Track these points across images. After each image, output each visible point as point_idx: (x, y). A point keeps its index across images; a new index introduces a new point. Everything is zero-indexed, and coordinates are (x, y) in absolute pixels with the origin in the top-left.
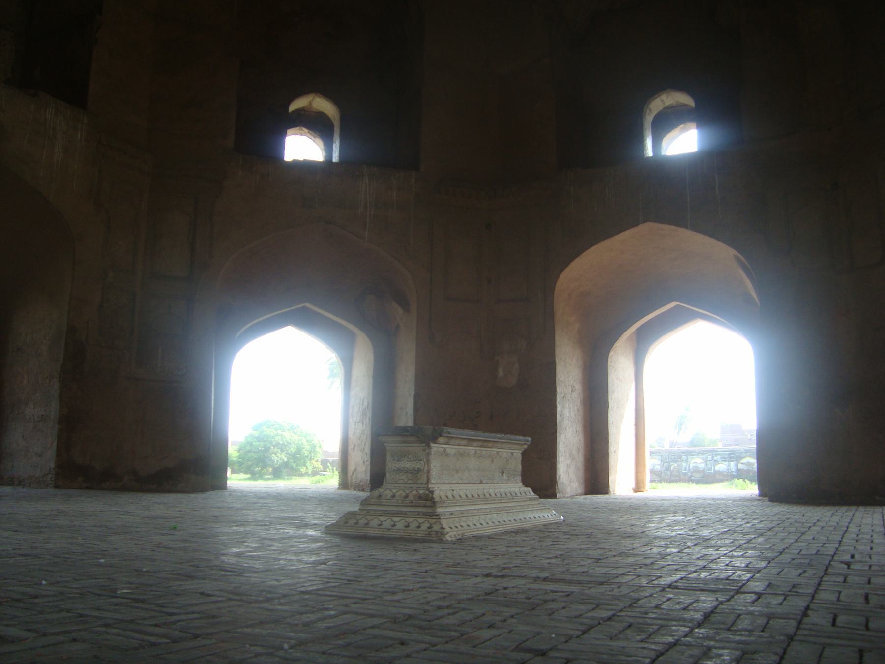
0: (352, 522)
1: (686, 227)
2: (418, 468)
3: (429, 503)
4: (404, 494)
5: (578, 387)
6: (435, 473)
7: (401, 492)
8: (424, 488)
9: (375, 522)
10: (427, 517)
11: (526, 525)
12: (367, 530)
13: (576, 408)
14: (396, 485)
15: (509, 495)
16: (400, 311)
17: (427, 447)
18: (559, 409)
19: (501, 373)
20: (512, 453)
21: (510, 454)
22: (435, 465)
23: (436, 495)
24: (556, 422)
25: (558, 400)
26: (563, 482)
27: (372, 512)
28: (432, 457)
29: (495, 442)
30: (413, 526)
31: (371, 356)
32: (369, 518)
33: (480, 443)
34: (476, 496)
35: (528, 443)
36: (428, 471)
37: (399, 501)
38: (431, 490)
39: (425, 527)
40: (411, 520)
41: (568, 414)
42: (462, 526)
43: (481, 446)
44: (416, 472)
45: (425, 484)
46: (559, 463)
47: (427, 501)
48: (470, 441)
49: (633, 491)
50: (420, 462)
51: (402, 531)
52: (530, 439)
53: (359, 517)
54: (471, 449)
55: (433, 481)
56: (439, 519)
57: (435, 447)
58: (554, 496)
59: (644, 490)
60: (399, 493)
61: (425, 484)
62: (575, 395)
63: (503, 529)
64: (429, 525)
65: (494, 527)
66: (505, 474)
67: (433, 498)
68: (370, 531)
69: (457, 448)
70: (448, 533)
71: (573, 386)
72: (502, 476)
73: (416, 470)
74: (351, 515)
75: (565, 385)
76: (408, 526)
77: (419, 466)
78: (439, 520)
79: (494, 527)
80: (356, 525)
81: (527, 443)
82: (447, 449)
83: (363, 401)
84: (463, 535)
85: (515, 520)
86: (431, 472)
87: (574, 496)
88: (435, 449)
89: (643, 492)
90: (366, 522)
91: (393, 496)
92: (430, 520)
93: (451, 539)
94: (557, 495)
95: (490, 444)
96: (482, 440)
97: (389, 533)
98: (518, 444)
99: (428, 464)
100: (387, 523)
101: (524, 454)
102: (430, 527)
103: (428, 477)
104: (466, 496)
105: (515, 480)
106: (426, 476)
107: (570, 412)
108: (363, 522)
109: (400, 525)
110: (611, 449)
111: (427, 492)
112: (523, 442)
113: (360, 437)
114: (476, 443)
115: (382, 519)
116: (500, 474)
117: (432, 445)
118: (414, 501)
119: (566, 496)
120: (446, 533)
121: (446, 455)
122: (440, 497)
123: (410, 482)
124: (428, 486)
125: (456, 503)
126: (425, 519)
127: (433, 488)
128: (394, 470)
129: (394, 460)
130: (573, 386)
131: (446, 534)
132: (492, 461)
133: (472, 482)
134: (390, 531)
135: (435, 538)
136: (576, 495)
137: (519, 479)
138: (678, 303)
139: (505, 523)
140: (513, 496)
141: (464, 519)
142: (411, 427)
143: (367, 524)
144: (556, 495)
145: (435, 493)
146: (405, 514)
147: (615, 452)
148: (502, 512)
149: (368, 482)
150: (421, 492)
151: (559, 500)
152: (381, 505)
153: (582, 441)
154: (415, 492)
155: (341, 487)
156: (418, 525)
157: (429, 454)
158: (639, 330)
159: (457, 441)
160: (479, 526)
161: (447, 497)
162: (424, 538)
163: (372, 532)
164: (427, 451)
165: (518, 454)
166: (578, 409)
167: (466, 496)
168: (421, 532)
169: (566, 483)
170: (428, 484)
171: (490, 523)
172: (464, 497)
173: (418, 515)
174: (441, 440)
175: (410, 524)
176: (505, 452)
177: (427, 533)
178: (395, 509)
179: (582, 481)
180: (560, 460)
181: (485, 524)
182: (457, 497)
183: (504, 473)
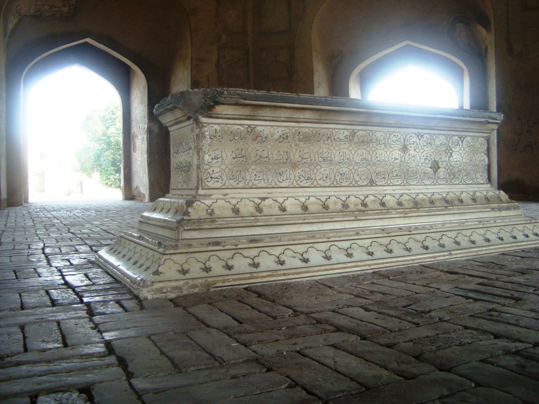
16: (484, 31)
28: (206, 142)
36: (198, 167)
69: (294, 127)
105: (472, 179)
117: (204, 120)
124: (197, 192)
157: (200, 137)
164: (197, 131)
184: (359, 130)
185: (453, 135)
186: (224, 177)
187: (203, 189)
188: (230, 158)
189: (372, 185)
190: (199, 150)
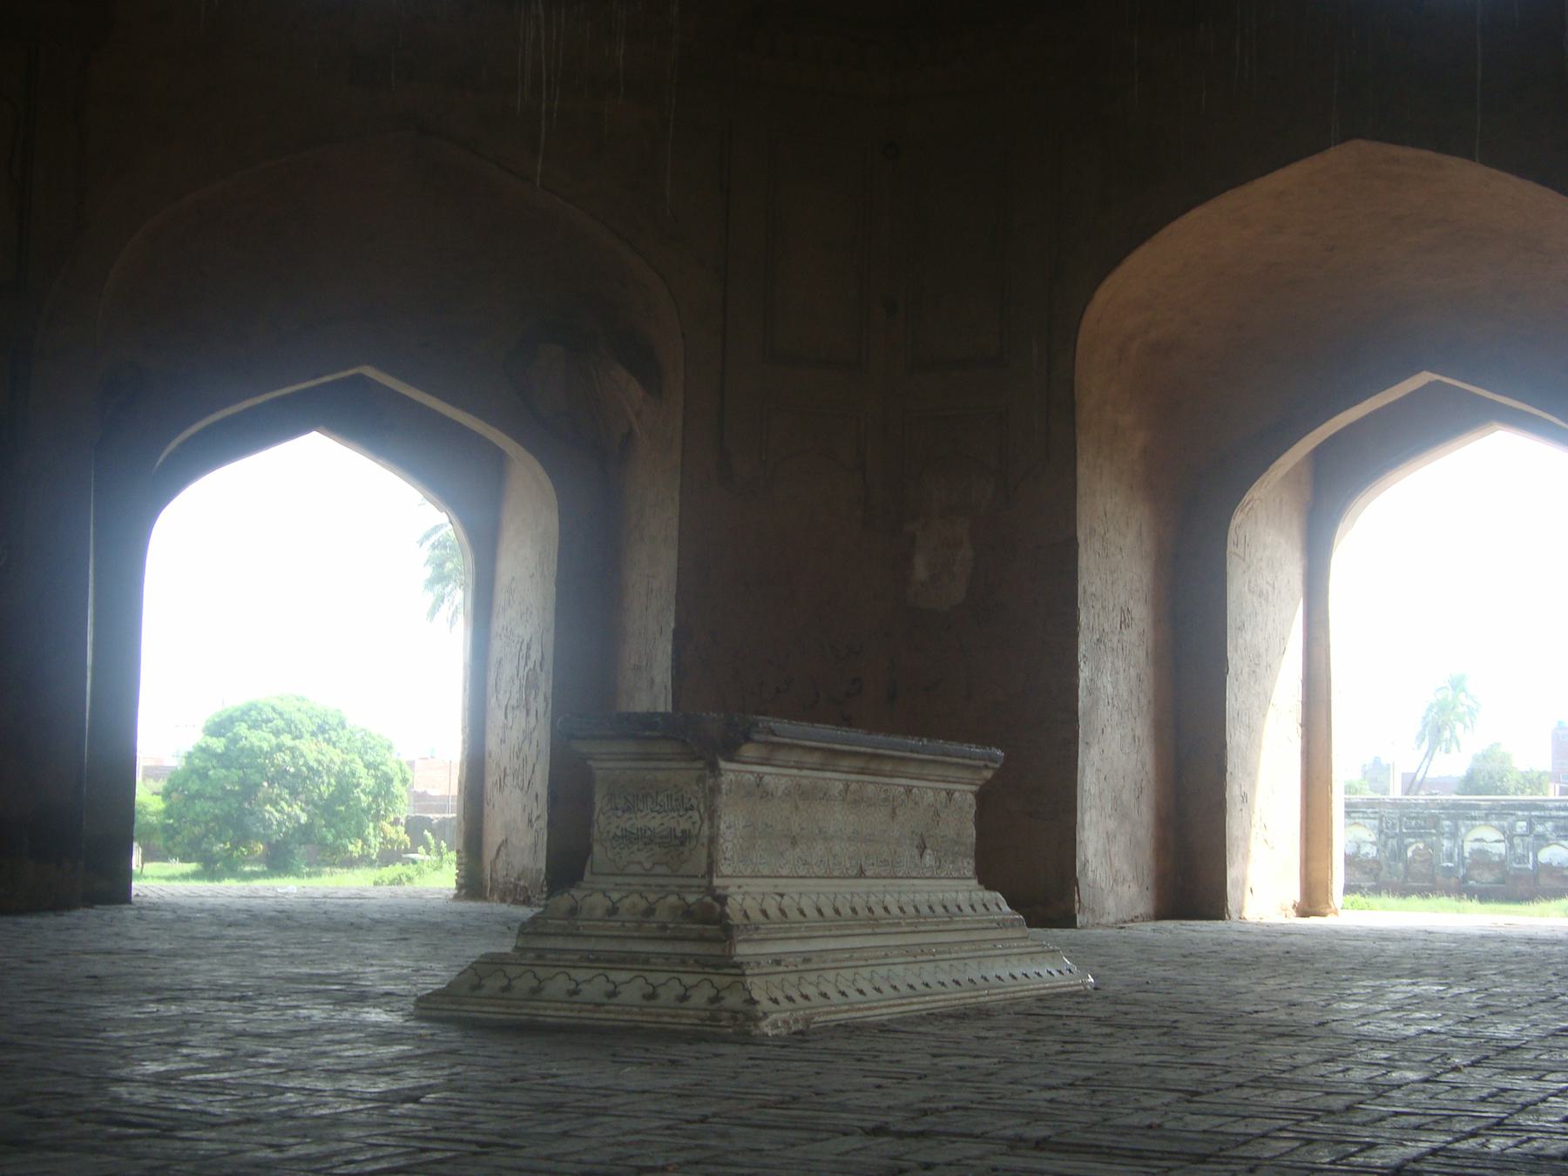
0: (493, 984)
1: (1469, 155)
2: (684, 831)
3: (712, 930)
4: (643, 904)
5: (1141, 613)
6: (730, 845)
7: (635, 898)
8: (699, 887)
9: (558, 985)
10: (707, 970)
11: (987, 999)
12: (537, 1008)
13: (1133, 672)
14: (619, 880)
15: (939, 910)
17: (707, 772)
18: (1084, 673)
19: (920, 571)
20: (950, 793)
21: (944, 794)
22: (732, 822)
23: (733, 908)
24: (1076, 713)
25: (1082, 648)
26: (1094, 881)
27: (550, 956)
28: (722, 800)
29: (902, 759)
30: (668, 995)
31: (550, 520)
32: (541, 972)
33: (859, 763)
34: (846, 911)
35: (997, 766)
36: (713, 840)
37: (627, 924)
38: (719, 891)
39: (700, 998)
40: (663, 977)
41: (1110, 689)
42: (806, 997)
43: (862, 772)
44: (677, 842)
45: (703, 877)
46: (1083, 825)
47: (708, 923)
48: (831, 757)
49: (1292, 913)
50: (690, 813)
51: (636, 1010)
52: (999, 753)
53: (512, 971)
54: (834, 781)
55: (725, 869)
56: (743, 975)
57: (733, 771)
58: (1068, 921)
59: (1328, 911)
60: (627, 902)
61: (703, 877)
62: (1131, 636)
63: (921, 1007)
64: (712, 992)
65: (899, 1001)
66: (928, 851)
67: (724, 916)
68: (546, 1008)
70: (766, 1015)
71: (1126, 611)
72: (921, 856)
73: (676, 837)
74: (493, 963)
75: (1104, 608)
76: (652, 996)
77: (684, 825)
78: (742, 979)
79: (899, 1001)
80: (505, 995)
81: (990, 764)
82: (766, 779)
83: (529, 648)
84: (808, 1020)
85: (957, 983)
86: (721, 841)
87: (1125, 922)
88: (731, 776)
89: (1323, 915)
90: (535, 983)
91: (613, 911)
92: (716, 979)
93: (775, 1032)
94: (1079, 918)
95: (888, 767)
96: (865, 754)
97: (597, 1015)
98: (969, 767)
99: (711, 818)
100: (594, 986)
101: (983, 797)
102: (716, 999)
103: (710, 855)
104: (820, 911)
105: (959, 870)
106: (704, 853)
107: (1115, 684)
108: (524, 984)
109: (632, 993)
110: (1233, 791)
111: (708, 899)
112: (982, 763)
113: (520, 749)
114: (845, 763)
115: (580, 975)
116: (916, 852)
117: (723, 764)
118: (671, 926)
119: (1103, 921)
120: (761, 1015)
121: (760, 791)
122: (745, 912)
123: (659, 870)
124: (711, 882)
125: (790, 929)
126: (702, 977)
127: (727, 887)
128: (615, 836)
129: (617, 809)
130: (1126, 611)
131: (760, 1019)
132: (894, 814)
133: (836, 873)
134: (602, 1008)
135: (730, 1030)
136: (1132, 921)
137: (968, 866)
138: (1437, 377)
139: (927, 990)
140: (951, 913)
141: (812, 977)
142: (664, 715)
143: (536, 991)
144: (1075, 917)
145: (730, 900)
146: (647, 962)
147: (1244, 798)
148: (919, 958)
149: (542, 877)
150: (691, 899)
151: (1084, 931)
152: (578, 936)
153: (1150, 767)
154: (672, 899)
155: (464, 891)
156: (681, 990)
157: (714, 791)
158: (1318, 453)
159: (794, 757)
160: (854, 996)
161: (764, 913)
162: (699, 1028)
163: (550, 1013)
164: (710, 782)
165: (965, 795)
166: (1138, 676)
167: (820, 911)
168: (691, 1013)
169: (1103, 886)
170: (711, 877)
171: (888, 991)
172: (811, 913)
173: (683, 963)
174: (749, 751)
175: (661, 990)
176: (928, 790)
177: (708, 1014)
178: (615, 946)
179: (1149, 881)
180: (1087, 818)
181: (871, 993)
182: (794, 915)
183: (925, 847)
184: (852, 782)
185: (942, 789)
186: (735, 857)
187: (717, 877)
188: (741, 827)
189: (860, 877)
190: (712, 814)
